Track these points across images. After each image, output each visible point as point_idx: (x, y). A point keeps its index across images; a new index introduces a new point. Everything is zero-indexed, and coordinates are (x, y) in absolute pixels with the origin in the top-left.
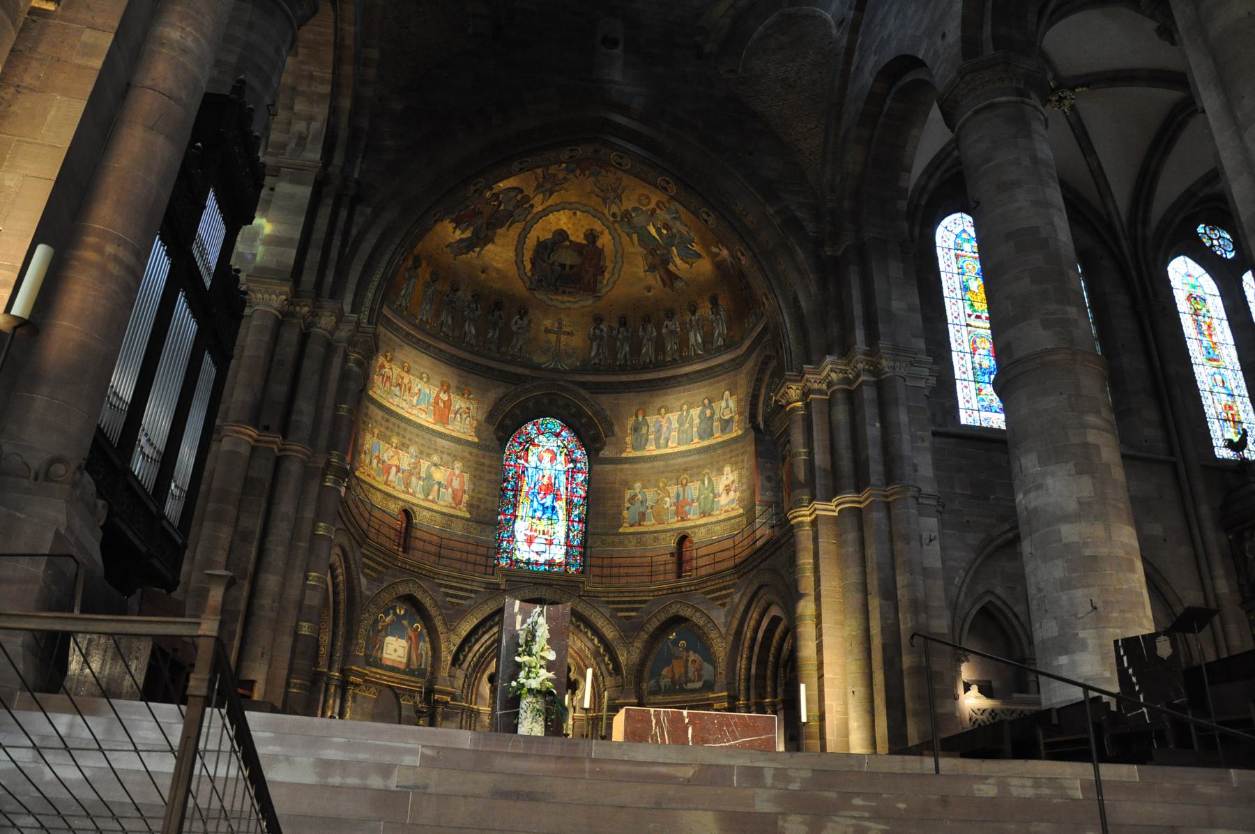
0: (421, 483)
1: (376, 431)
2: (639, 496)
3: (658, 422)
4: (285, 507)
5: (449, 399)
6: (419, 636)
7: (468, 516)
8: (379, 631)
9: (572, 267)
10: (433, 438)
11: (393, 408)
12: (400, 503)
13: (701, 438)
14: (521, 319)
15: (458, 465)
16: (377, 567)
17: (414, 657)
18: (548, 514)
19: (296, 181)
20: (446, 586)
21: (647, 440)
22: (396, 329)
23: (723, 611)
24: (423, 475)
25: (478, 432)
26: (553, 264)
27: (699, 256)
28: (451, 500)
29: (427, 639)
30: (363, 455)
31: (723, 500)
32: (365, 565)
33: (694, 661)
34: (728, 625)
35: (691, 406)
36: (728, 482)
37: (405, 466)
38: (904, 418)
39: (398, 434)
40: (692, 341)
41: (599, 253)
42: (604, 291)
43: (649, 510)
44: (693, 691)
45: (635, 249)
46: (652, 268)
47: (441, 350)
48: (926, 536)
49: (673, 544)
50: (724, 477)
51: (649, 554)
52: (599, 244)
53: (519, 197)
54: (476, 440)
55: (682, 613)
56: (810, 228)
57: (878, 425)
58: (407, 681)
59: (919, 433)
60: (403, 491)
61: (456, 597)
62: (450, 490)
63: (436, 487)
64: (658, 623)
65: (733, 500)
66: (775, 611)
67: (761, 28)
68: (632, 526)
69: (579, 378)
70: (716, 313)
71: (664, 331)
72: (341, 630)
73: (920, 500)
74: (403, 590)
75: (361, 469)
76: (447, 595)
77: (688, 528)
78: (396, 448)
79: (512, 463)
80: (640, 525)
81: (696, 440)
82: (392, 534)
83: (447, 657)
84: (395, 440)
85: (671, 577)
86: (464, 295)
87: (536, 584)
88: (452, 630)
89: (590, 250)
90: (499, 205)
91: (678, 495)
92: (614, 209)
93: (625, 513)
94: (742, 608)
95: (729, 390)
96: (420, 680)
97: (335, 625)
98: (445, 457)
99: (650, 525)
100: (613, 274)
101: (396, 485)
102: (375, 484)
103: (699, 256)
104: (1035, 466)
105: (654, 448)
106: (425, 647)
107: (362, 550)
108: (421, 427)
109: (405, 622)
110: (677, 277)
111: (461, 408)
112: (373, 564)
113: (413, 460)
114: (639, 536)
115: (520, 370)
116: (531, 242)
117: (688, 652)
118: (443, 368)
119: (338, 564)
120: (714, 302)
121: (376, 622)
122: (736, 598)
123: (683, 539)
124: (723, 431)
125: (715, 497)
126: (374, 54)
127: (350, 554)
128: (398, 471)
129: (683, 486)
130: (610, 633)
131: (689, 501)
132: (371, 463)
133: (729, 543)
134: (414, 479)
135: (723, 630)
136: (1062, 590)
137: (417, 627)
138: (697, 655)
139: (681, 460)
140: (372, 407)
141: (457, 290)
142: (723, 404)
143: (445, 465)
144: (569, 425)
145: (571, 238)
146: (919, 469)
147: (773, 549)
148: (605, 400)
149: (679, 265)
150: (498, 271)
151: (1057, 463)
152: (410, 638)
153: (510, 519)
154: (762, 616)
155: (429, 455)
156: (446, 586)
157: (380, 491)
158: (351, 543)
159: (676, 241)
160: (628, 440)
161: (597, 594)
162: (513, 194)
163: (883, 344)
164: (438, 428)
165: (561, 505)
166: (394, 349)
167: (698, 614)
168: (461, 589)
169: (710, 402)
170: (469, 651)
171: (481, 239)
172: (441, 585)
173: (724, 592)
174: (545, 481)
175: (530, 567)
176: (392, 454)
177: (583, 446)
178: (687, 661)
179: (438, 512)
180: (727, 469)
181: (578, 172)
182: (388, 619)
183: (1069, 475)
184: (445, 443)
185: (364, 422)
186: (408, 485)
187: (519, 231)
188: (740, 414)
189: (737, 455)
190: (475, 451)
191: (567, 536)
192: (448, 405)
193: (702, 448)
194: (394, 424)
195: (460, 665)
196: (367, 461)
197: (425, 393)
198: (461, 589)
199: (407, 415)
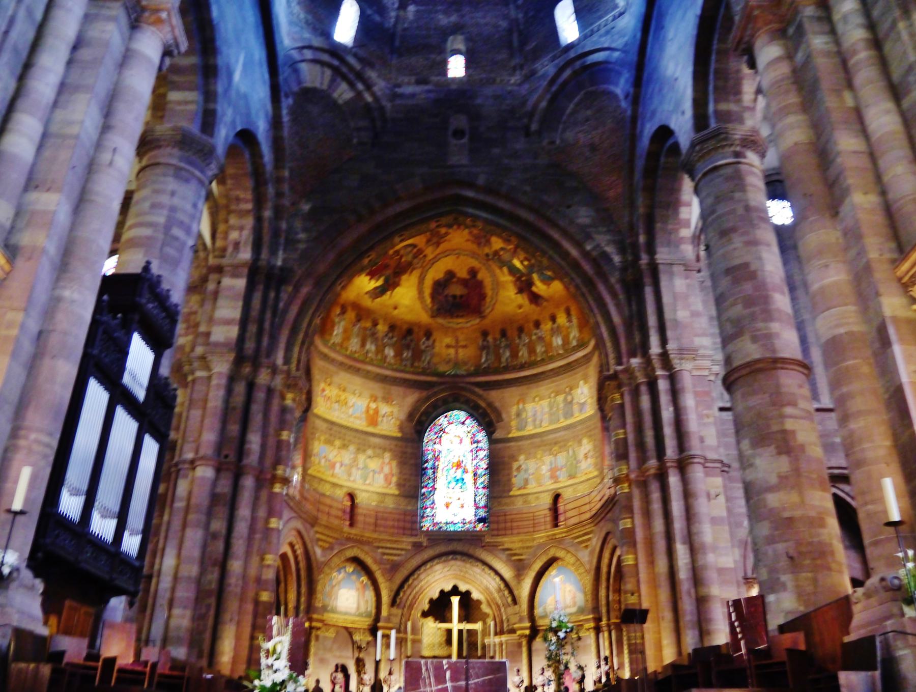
0: (360, 472)
6: (364, 587)
7: (397, 492)
9: (461, 296)
13: (566, 418)
15: (387, 456)
18: (460, 484)
19: (235, 275)
20: (382, 548)
21: (526, 422)
22: (332, 361)
23: (587, 552)
25: (401, 428)
32: (319, 540)
33: (570, 591)
34: (590, 562)
35: (557, 394)
36: (586, 451)
39: (340, 438)
40: (555, 344)
41: (480, 285)
42: (488, 311)
45: (505, 278)
46: (520, 291)
47: (368, 372)
48: (713, 492)
50: (583, 448)
51: (532, 510)
52: (480, 276)
53: (415, 250)
54: (399, 435)
56: (617, 259)
61: (391, 555)
63: (371, 474)
65: (590, 464)
66: (618, 552)
67: (572, 106)
68: (520, 489)
70: (570, 321)
73: (707, 465)
74: (350, 553)
76: (384, 554)
78: (339, 448)
80: (524, 488)
81: (562, 420)
82: (340, 514)
83: (386, 599)
84: (338, 443)
85: (548, 526)
86: (382, 328)
89: (473, 283)
92: (487, 250)
98: (378, 451)
102: (324, 477)
106: (370, 594)
108: (357, 431)
109: (354, 577)
111: (386, 413)
113: (352, 456)
114: (524, 497)
121: (331, 579)
122: (594, 541)
123: (557, 497)
124: (581, 410)
125: (577, 463)
126: (286, 173)
128: (342, 465)
130: (507, 573)
131: (559, 467)
132: (319, 463)
133: (587, 500)
134: (354, 470)
137: (363, 581)
139: (551, 436)
143: (377, 456)
144: (471, 416)
147: (611, 506)
148: (494, 396)
149: (540, 287)
152: (358, 589)
153: (431, 491)
154: (612, 554)
155: (364, 451)
156: (382, 548)
162: (410, 249)
163: (671, 346)
164: (371, 429)
165: (469, 478)
168: (394, 549)
171: (390, 285)
172: (378, 547)
173: (586, 537)
174: (456, 460)
175: (448, 526)
179: (373, 492)
184: (377, 441)
186: (350, 475)
187: (418, 275)
188: (592, 398)
189: (590, 431)
190: (400, 443)
191: (475, 500)
192: (376, 411)
198: (394, 549)
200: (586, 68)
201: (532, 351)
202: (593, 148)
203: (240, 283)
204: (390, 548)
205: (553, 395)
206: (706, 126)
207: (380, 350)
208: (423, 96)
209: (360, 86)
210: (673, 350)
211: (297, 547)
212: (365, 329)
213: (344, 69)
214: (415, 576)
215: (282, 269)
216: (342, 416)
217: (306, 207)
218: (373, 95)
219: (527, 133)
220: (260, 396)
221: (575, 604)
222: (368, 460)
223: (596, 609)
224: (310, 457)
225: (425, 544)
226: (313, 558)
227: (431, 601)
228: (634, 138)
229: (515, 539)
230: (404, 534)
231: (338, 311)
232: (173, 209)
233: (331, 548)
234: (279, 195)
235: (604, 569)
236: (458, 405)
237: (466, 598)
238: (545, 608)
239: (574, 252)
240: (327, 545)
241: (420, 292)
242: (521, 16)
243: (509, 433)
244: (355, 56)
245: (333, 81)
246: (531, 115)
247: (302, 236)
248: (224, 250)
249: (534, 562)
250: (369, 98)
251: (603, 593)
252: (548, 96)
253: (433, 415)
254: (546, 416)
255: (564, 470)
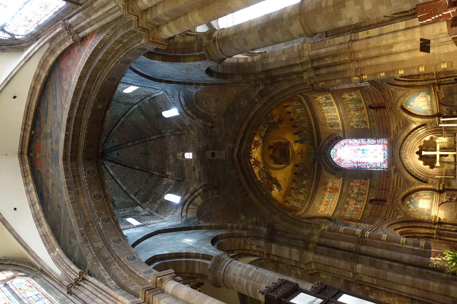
0: (359, 196)
1: (344, 213)
2: (356, 123)
3: (329, 120)
4: (379, 251)
5: (329, 188)
8: (417, 210)
9: (280, 152)
10: (343, 193)
11: (335, 207)
12: (368, 203)
14: (299, 166)
15: (351, 184)
16: (393, 212)
17: (426, 197)
19: (271, 248)
20: (397, 187)
21: (335, 122)
23: (398, 92)
24: (357, 196)
25: (339, 178)
26: (280, 158)
27: (272, 114)
28: (364, 186)
29: (418, 192)
30: (353, 217)
31: (355, 96)
32: (393, 217)
34: (403, 90)
35: (322, 110)
36: (348, 96)
37: (354, 202)
38: (323, 50)
39: (344, 205)
40: (300, 112)
41: (275, 144)
42: (287, 141)
43: (361, 119)
44: (431, 98)
47: (313, 191)
49: (372, 111)
50: (346, 97)
52: (272, 144)
53: (261, 171)
54: (342, 178)
55: (400, 106)
56: (261, 88)
57: (326, 59)
58: (436, 199)
59: (328, 44)
60: (363, 203)
61: (400, 183)
62: (361, 186)
63: (360, 191)
64: (404, 113)
68: (367, 125)
69: (316, 146)
70: (290, 106)
71: (297, 121)
72: (419, 225)
74: (400, 202)
75: (358, 218)
76: (400, 186)
77: (366, 107)
79: (348, 165)
80: (366, 122)
83: (424, 186)
85: (385, 111)
87: (393, 156)
88: (414, 184)
90: (265, 177)
91: (354, 111)
92: (261, 142)
93: (362, 127)
94: (396, 87)
95: (315, 99)
96: (435, 195)
97: (417, 227)
98: (349, 188)
99: (366, 119)
100: (281, 139)
101: (361, 205)
102: (362, 213)
103: (272, 114)
104: (343, 22)
105: (338, 120)
106: (421, 193)
107: (387, 218)
108: (340, 197)
109: (412, 201)
110: (279, 119)
112: (392, 214)
115: (316, 165)
116: (275, 166)
117: (415, 101)
118: (319, 190)
119: (394, 228)
120: (286, 107)
121: (413, 211)
123: (370, 107)
124: (330, 99)
125: (354, 99)
127: (389, 224)
128: (356, 205)
129: (351, 109)
132: (355, 214)
134: (359, 199)
135: (405, 91)
136: (391, 5)
137: (414, 196)
138: (416, 98)
139: (342, 111)
140: (336, 215)
141: (293, 187)
142: (320, 100)
145: (271, 153)
146: (341, 42)
148: (323, 137)
149: (276, 119)
150: (285, 175)
151: (341, 15)
152: (418, 199)
154: (399, 80)
155: (349, 194)
157: (364, 211)
158: (386, 223)
159: (268, 121)
160: (336, 128)
161: (394, 135)
163: (298, 62)
164: (339, 191)
165: (362, 147)
166: (315, 207)
167: (400, 100)
168: (397, 182)
169: (320, 104)
170: (421, 177)
172: (397, 189)
173: (391, 93)
176: (351, 207)
177: (339, 141)
178: (419, 101)
179: (369, 191)
180: (343, 96)
181: (251, 155)
182: (412, 207)
183: (346, 10)
185: (341, 217)
188: (323, 95)
191: (373, 144)
192: (331, 188)
193: (336, 105)
194: (340, 207)
195: (427, 180)
196: (354, 215)
197: (328, 196)
198: (397, 182)
199: (337, 202)
200: (187, 105)
201: (303, 121)
202: (217, 100)
203: (274, 246)
204: (397, 183)
205: (323, 112)
206: (204, 55)
207: (304, 186)
208: (199, 169)
209: (196, 194)
210: (299, 61)
211: (396, 227)
212: (295, 192)
213: (190, 200)
214: (411, 171)
215: (268, 228)
216: (333, 203)
217: (243, 217)
218: (199, 189)
219: (213, 127)
220: (323, 240)
221: (425, 96)
222: (354, 192)
223: (428, 86)
224: (353, 218)
225: (395, 167)
226: (402, 220)
227: (425, 164)
228: (213, 84)
229: (392, 125)
230: (390, 177)
231: (287, 204)
232: (241, 275)
233: (397, 211)
234: (238, 228)
235: (407, 83)
236: (328, 153)
237: (422, 149)
238: (428, 110)
239: (259, 106)
240: (396, 213)
241: (279, 169)
242: (169, 131)
243: (341, 130)
244: (185, 195)
245: (194, 205)
246: (205, 126)
247: (254, 219)
248: (260, 252)
249: (403, 116)
250: (201, 190)
251: (419, 83)
252: (198, 119)
253: (333, 163)
254: (332, 114)
255: (357, 105)
